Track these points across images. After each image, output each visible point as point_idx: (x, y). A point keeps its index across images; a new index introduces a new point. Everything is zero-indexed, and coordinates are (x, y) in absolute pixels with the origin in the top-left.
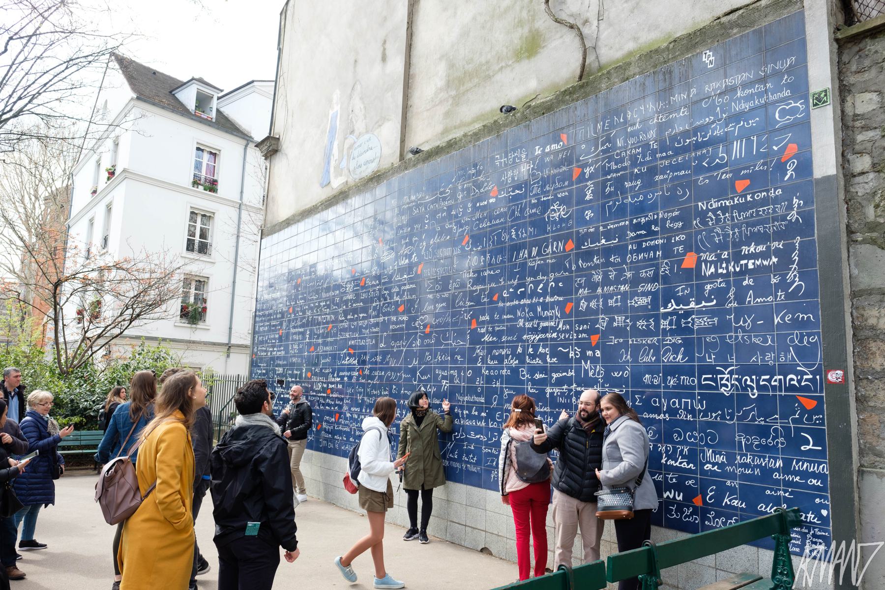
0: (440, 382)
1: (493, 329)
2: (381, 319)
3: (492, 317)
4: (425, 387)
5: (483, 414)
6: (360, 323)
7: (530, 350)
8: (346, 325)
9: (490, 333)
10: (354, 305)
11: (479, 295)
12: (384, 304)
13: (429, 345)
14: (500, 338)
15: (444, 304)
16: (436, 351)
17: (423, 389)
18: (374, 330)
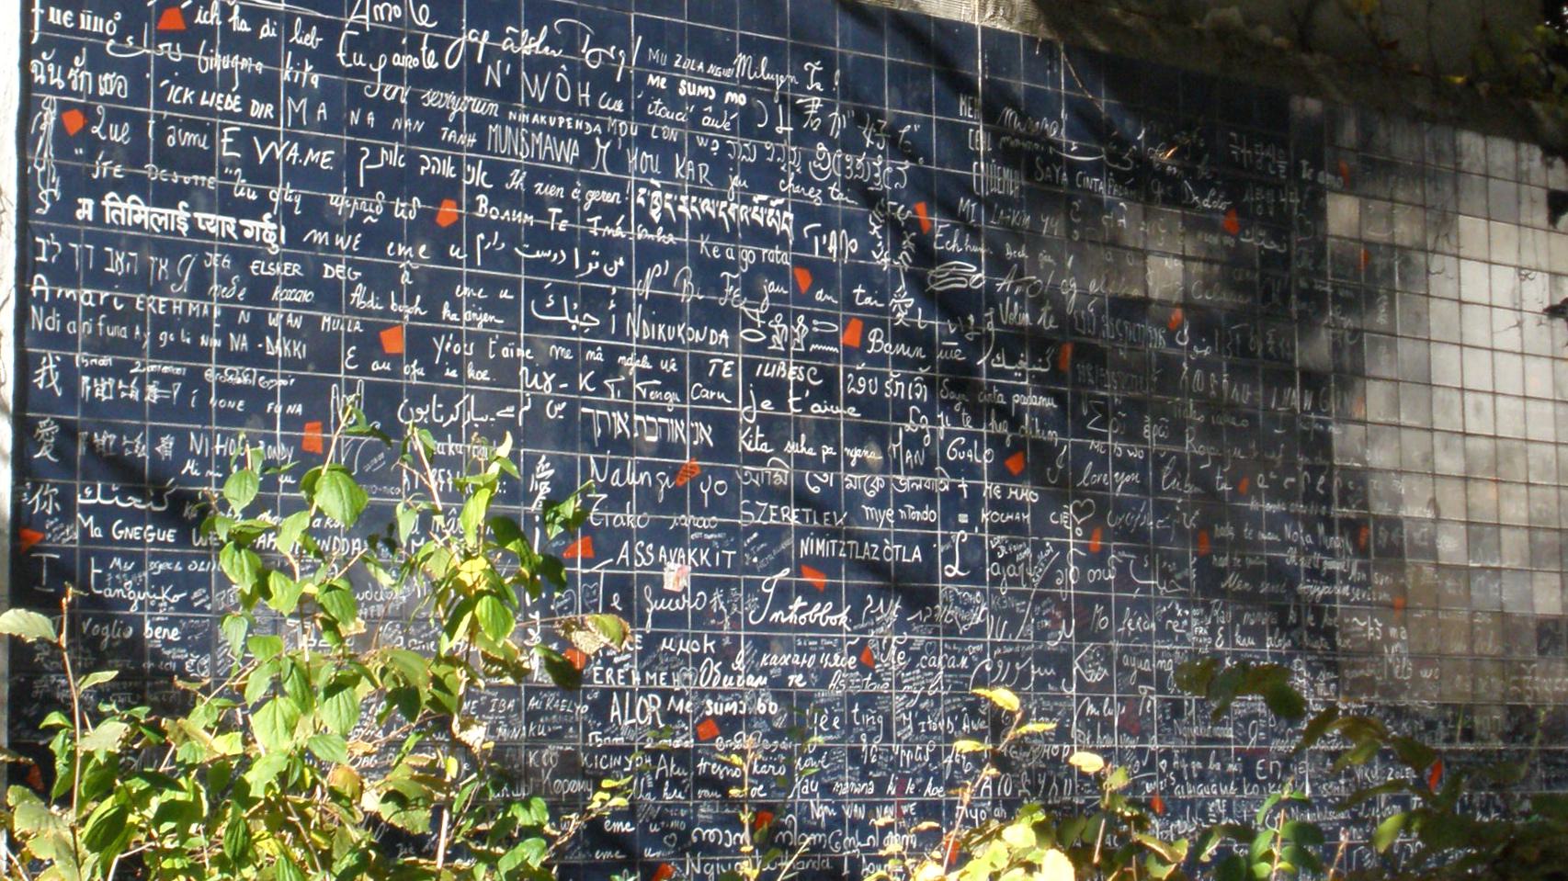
0: (1134, 689)
1: (1243, 562)
2: (943, 484)
3: (1239, 532)
4: (1098, 703)
5: (1232, 768)
6: (852, 481)
7: (1310, 618)
8: (781, 474)
9: (1238, 570)
10: (816, 408)
11: (1212, 471)
12: (950, 435)
13: (1102, 585)
14: (1256, 586)
15: (1135, 477)
16: (1121, 603)
17: (1091, 709)
18: (916, 515)
